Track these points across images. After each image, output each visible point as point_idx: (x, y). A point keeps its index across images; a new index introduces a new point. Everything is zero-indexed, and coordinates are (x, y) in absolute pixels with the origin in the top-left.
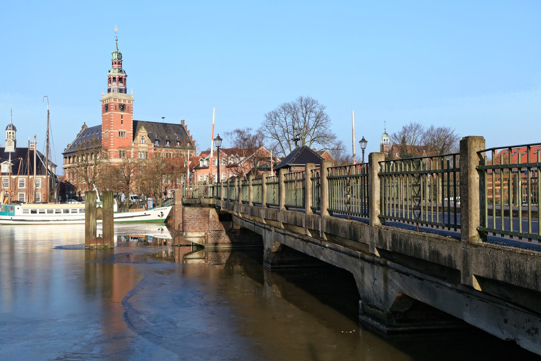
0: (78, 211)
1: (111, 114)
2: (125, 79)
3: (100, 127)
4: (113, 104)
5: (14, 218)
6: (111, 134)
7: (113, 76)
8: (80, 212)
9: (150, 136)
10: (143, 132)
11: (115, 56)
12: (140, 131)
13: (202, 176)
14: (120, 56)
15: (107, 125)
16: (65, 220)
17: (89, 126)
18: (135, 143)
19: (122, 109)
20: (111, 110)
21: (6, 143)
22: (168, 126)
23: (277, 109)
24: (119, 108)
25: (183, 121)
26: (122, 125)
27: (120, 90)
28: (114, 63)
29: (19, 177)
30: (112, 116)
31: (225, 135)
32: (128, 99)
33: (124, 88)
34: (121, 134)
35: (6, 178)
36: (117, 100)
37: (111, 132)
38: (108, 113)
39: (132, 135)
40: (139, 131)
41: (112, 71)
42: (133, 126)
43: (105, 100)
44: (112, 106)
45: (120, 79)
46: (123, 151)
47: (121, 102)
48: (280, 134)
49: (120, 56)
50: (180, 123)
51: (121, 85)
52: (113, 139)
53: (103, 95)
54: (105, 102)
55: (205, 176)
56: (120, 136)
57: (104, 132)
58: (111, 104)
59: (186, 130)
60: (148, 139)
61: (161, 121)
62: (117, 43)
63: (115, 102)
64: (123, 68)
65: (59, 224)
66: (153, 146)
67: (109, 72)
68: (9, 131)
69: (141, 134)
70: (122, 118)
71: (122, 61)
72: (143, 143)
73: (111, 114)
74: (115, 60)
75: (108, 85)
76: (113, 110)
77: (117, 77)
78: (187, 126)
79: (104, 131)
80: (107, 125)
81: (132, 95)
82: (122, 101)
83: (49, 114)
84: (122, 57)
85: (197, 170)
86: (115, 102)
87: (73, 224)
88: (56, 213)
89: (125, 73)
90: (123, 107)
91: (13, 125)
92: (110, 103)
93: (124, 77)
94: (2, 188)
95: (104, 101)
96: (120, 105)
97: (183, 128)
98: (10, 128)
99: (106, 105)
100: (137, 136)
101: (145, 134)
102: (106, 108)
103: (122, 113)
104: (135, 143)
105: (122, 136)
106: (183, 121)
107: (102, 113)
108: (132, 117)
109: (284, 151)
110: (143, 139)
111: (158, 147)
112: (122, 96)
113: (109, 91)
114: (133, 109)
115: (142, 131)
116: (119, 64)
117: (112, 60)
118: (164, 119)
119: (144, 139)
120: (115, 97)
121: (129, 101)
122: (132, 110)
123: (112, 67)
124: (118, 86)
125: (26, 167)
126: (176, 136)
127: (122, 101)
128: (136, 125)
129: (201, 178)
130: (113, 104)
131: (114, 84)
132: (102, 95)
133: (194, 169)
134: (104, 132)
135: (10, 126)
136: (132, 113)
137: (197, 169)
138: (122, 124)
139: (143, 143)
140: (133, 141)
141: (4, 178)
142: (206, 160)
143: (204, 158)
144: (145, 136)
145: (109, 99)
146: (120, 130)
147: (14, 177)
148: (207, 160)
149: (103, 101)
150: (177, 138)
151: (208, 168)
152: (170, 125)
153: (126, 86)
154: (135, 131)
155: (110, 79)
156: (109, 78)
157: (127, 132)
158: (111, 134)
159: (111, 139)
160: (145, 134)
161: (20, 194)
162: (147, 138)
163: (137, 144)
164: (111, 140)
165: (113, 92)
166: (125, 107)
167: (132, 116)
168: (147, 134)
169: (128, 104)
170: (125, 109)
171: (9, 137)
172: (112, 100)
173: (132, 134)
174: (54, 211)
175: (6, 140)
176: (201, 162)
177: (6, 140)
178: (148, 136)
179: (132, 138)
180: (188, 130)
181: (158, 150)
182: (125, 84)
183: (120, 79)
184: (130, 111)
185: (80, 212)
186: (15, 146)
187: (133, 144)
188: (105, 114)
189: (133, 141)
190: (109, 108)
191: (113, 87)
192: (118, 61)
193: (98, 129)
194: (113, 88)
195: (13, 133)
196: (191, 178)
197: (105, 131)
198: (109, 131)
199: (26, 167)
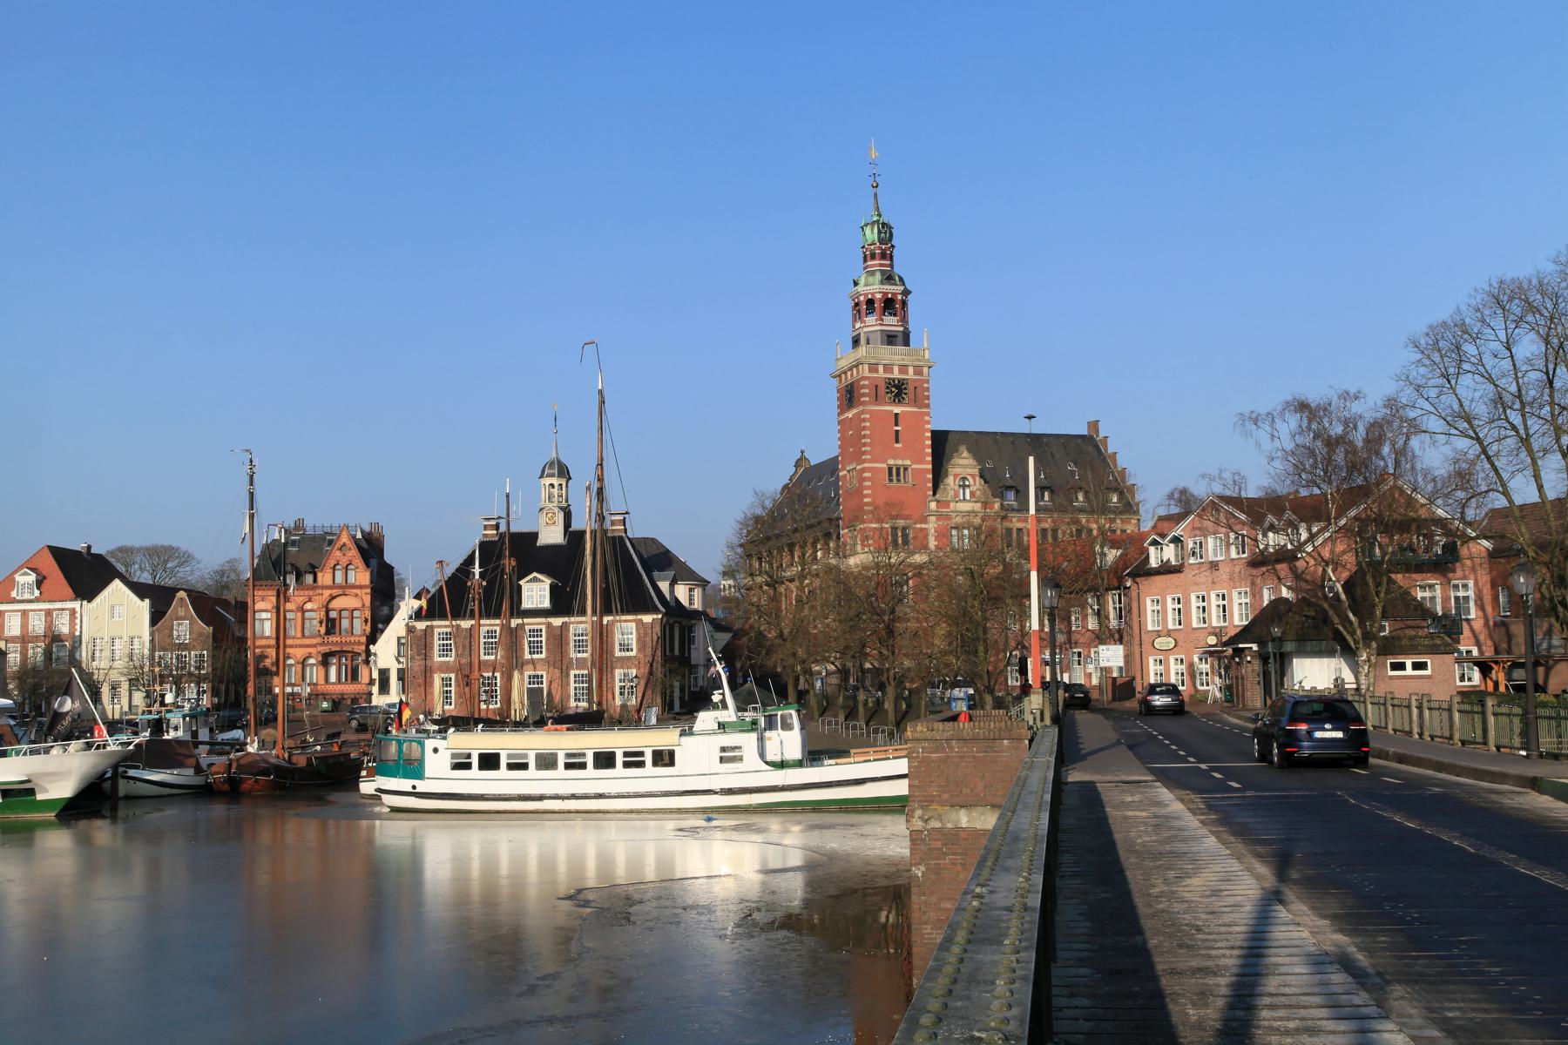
0: (648, 758)
1: (863, 412)
2: (904, 303)
3: (834, 461)
4: (867, 383)
5: (422, 786)
6: (866, 475)
7: (866, 295)
8: (655, 764)
9: (987, 475)
10: (963, 465)
11: (872, 235)
12: (956, 461)
13: (1158, 601)
14: (885, 233)
15: (851, 450)
16: (600, 796)
17: (815, 460)
18: (938, 501)
19: (896, 396)
20: (862, 399)
21: (543, 519)
22: (1047, 443)
23: (1464, 308)
24: (888, 393)
25: (1094, 425)
26: (896, 445)
27: (889, 336)
28: (869, 257)
29: (572, 623)
30: (864, 420)
31: (1243, 425)
32: (916, 363)
33: (902, 329)
34: (895, 473)
35: (536, 627)
36: (881, 368)
37: (864, 470)
38: (855, 411)
39: (930, 476)
40: (953, 462)
41: (862, 281)
42: (933, 446)
43: (845, 373)
44: (864, 387)
45: (889, 305)
46: (904, 529)
47: (892, 372)
48: (1481, 410)
49: (885, 233)
50: (1084, 431)
51: (892, 323)
52: (869, 492)
53: (839, 357)
54: (846, 378)
55: (1169, 600)
56: (891, 480)
57: (845, 472)
58: (861, 383)
59: (1106, 450)
60: (980, 485)
61: (1024, 427)
63: (875, 375)
64: (899, 269)
65: (578, 812)
66: (997, 506)
67: (856, 284)
68: (548, 481)
69: (958, 470)
70: (896, 425)
71: (893, 246)
72: (964, 499)
73: (863, 412)
74: (872, 247)
75: (854, 327)
76: (867, 399)
77: (879, 296)
78: (1107, 437)
79: (844, 469)
80: (851, 450)
81: (927, 352)
82: (896, 369)
83: (604, 402)
84: (891, 235)
85: (1138, 580)
86: (875, 375)
87: (631, 812)
88: (568, 766)
89: (904, 284)
90: (898, 390)
91: (559, 462)
92: (859, 380)
93: (900, 297)
94: (527, 656)
95: (843, 376)
96: (890, 383)
97: (1096, 447)
98: (551, 471)
99: (847, 386)
100: (947, 476)
101: (969, 471)
102: (849, 396)
103: (897, 410)
104: (938, 501)
105: (899, 480)
106: (1094, 425)
107: (839, 414)
108: (927, 418)
109: (1504, 485)
110: (964, 487)
111: (1013, 510)
112: (894, 355)
113: (856, 342)
114: (932, 393)
115: (962, 462)
116: (883, 256)
117: (863, 247)
118: (1033, 419)
119: (969, 486)
120: (873, 358)
121: (918, 371)
122: (928, 398)
123: (865, 269)
124: (881, 325)
125: (653, 593)
126: (1072, 472)
127: (896, 369)
128: (942, 444)
129: (1156, 608)
130: (867, 383)
131: (871, 320)
132: (838, 359)
133: (1127, 575)
134: (845, 472)
135: (551, 464)
136: (928, 406)
137: (1140, 576)
138: (897, 441)
139: (964, 499)
140: (934, 494)
141: (532, 627)
142: (1172, 541)
143: (1163, 536)
144: (973, 476)
145: (857, 366)
146: (891, 462)
147: (557, 622)
148: (1176, 540)
149: (839, 376)
150: (1077, 477)
151: (1177, 570)
152: (1051, 439)
153: (907, 322)
154: (942, 464)
155: (857, 308)
156: (857, 304)
157: (914, 466)
158: (866, 475)
159: (865, 492)
160: (969, 471)
161: (575, 676)
162: (976, 484)
163: (947, 505)
164: (866, 496)
165: (868, 343)
166: (905, 389)
167: (928, 414)
168: (976, 471)
169: (914, 380)
170: (906, 394)
171: (549, 498)
172: (865, 371)
173: (931, 471)
174: (561, 761)
175: (541, 509)
176: (1152, 550)
177: (541, 509)
178: (981, 476)
179: (930, 485)
180: (1110, 450)
181: (1014, 520)
182: (904, 319)
183: (889, 305)
184: (920, 399)
185: (655, 764)
186: (567, 524)
187: (933, 505)
188: (846, 415)
189: (934, 494)
190: (855, 394)
191: (865, 330)
192: (880, 248)
193: (831, 466)
194: (866, 332)
195: (560, 485)
196: (1120, 608)
197: (848, 469)
198: (859, 467)
199: (653, 593)
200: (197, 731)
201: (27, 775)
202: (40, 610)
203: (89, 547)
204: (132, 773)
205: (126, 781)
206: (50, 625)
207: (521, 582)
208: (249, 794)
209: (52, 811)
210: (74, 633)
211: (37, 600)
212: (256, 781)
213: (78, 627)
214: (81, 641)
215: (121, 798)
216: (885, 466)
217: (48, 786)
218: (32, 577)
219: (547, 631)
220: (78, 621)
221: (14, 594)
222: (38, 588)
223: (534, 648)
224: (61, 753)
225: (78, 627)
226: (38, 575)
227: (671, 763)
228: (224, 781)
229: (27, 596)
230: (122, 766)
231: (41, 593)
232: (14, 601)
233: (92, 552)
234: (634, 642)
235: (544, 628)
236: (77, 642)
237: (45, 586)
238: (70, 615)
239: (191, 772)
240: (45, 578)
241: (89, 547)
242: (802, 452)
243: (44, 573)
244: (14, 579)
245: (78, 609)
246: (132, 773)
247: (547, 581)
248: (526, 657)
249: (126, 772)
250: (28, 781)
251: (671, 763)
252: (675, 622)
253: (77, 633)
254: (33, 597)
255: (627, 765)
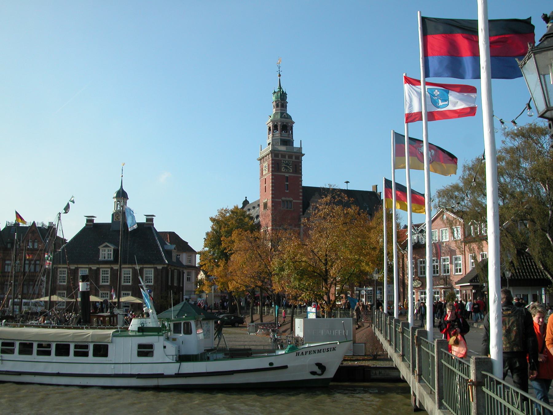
35: (105, 269)
40: (312, 199)
50: (371, 189)
51: (285, 136)
61: (344, 187)
62: (280, 79)
86: (277, 159)
141: (104, 269)
147: (116, 267)
157: (294, 201)
179: (301, 210)
207: (100, 247)
216: (280, 200)
219: (111, 272)
223: (104, 279)
227: (105, 355)
234: (153, 278)
235: (109, 270)
242: (246, 197)
247: (112, 247)
248: (100, 284)
251: (105, 355)
252: (174, 269)
255: (77, 354)
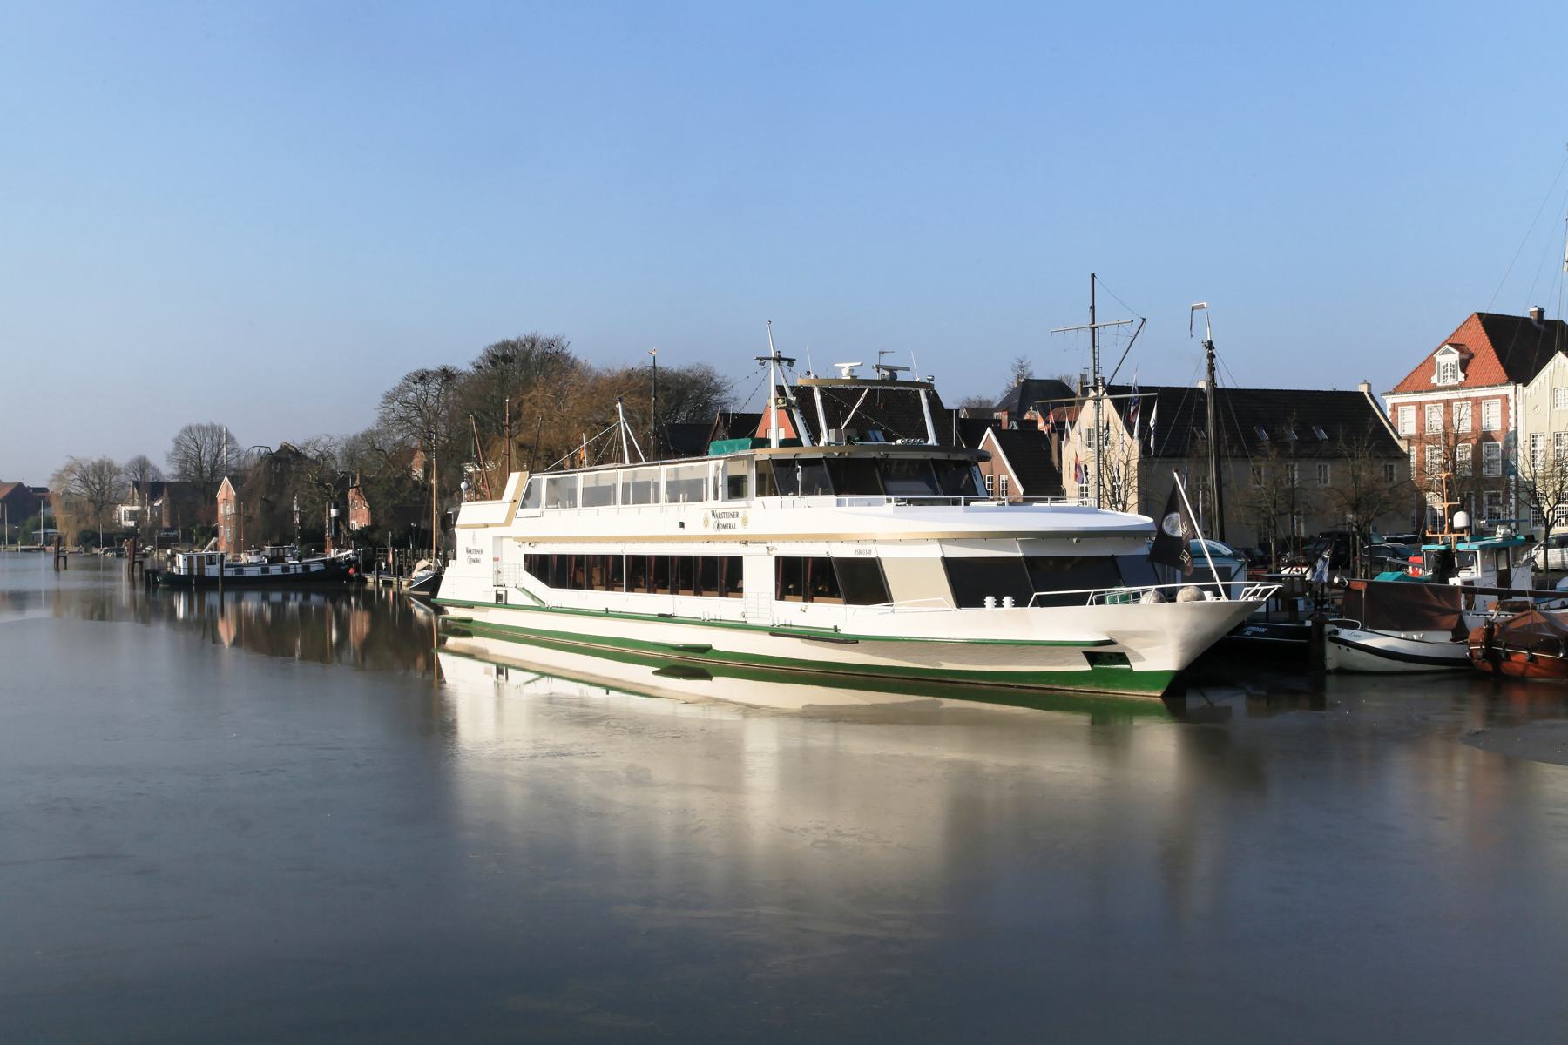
200: (1507, 572)
201: (1108, 634)
202: (1438, 401)
203: (1541, 312)
204: (1345, 634)
205: (1336, 645)
206: (1448, 424)
208: (1520, 680)
209: (1156, 689)
210: (1507, 428)
211: (1461, 386)
212: (1533, 659)
213: (1512, 421)
214: (1516, 439)
215: (1330, 672)
217: (1142, 652)
218: (1454, 357)
220: (1512, 412)
221: (1434, 380)
222: (1463, 370)
224: (1152, 602)
225: (1512, 421)
226: (1461, 352)
228: (1484, 656)
229: (1451, 382)
230: (1332, 623)
231: (1466, 377)
232: (1435, 389)
233: (1545, 318)
236: (1511, 439)
237: (1471, 368)
238: (1445, 407)
239: (1445, 637)
240: (1472, 356)
241: (1541, 312)
243: (1472, 349)
244: (1435, 359)
245: (1511, 396)
246: (1345, 634)
249: (1336, 632)
250: (1110, 643)
253: (1512, 429)
254: (1457, 383)
